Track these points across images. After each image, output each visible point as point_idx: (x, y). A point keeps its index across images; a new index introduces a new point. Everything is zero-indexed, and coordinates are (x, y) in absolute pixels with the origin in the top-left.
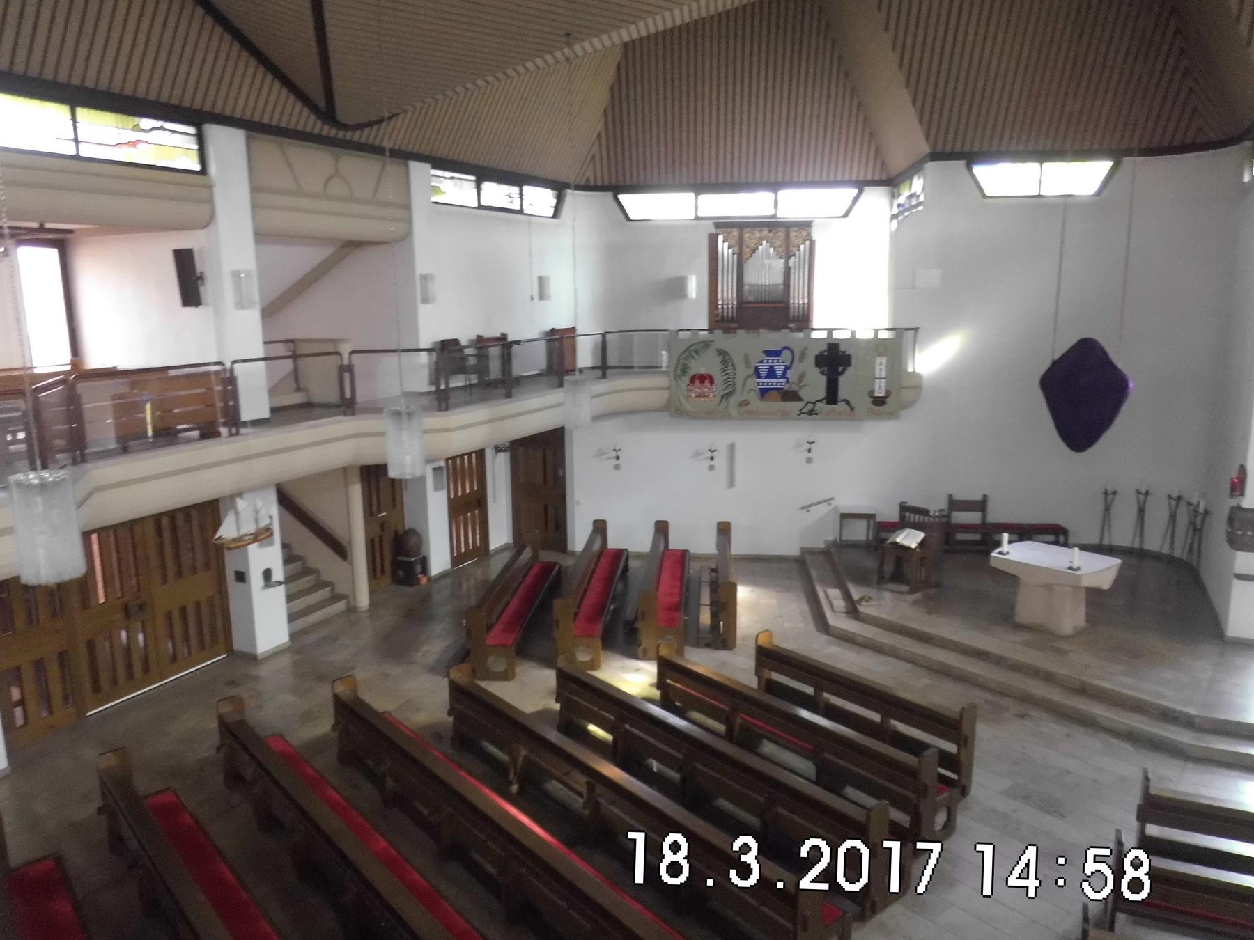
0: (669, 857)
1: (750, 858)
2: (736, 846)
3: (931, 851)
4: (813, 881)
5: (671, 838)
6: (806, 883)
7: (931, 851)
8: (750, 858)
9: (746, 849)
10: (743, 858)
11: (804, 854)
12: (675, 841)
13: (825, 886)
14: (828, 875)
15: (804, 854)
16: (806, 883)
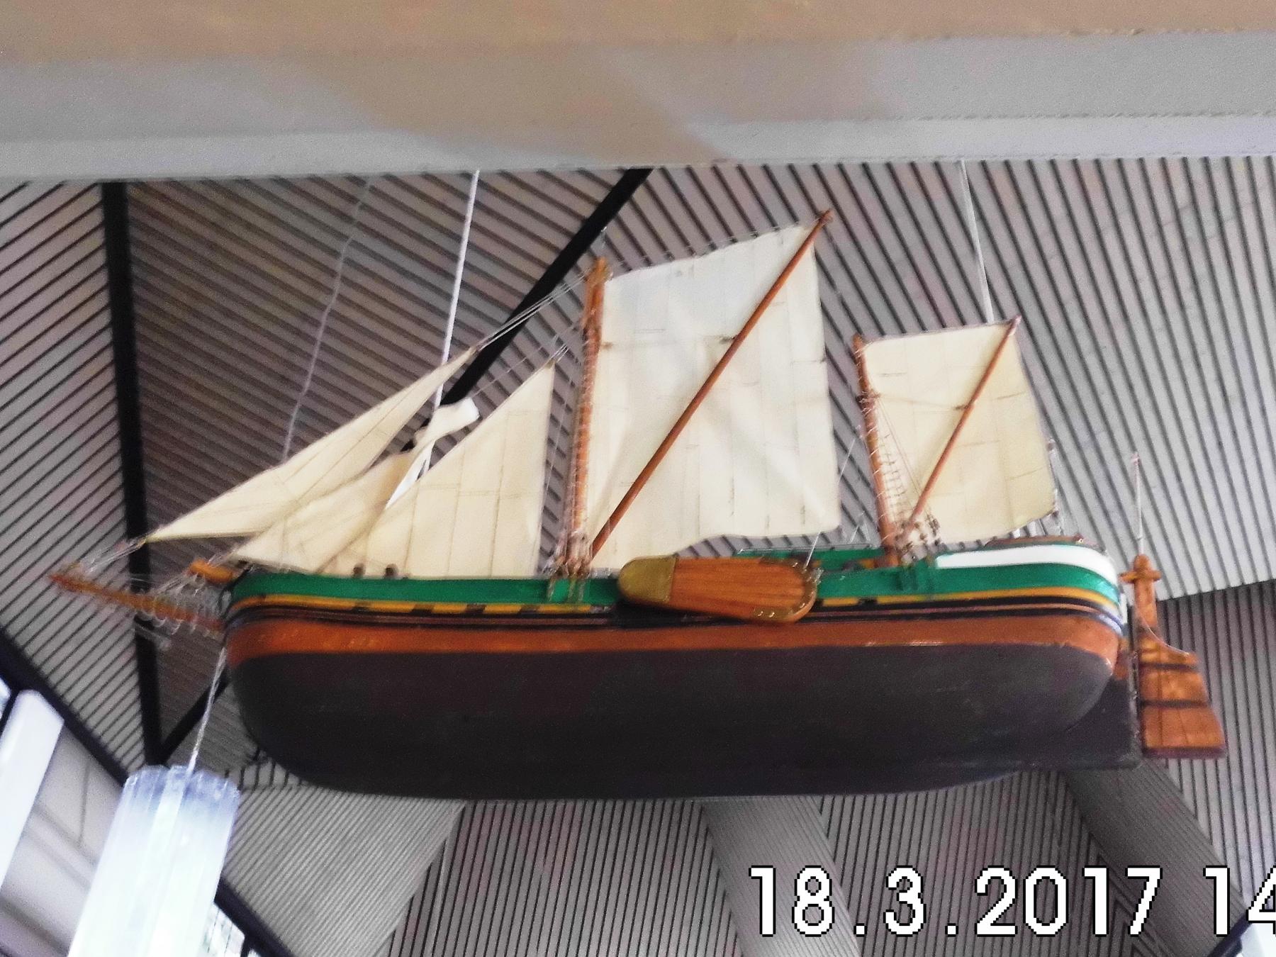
0: (806, 899)
1: (911, 897)
2: (893, 882)
3: (1147, 879)
4: (994, 924)
5: (807, 874)
6: (985, 927)
7: (1147, 879)
8: (911, 897)
9: (905, 884)
10: (903, 897)
11: (981, 889)
12: (813, 878)
13: (1010, 930)
14: (1014, 915)
15: (981, 889)
16: (985, 927)
